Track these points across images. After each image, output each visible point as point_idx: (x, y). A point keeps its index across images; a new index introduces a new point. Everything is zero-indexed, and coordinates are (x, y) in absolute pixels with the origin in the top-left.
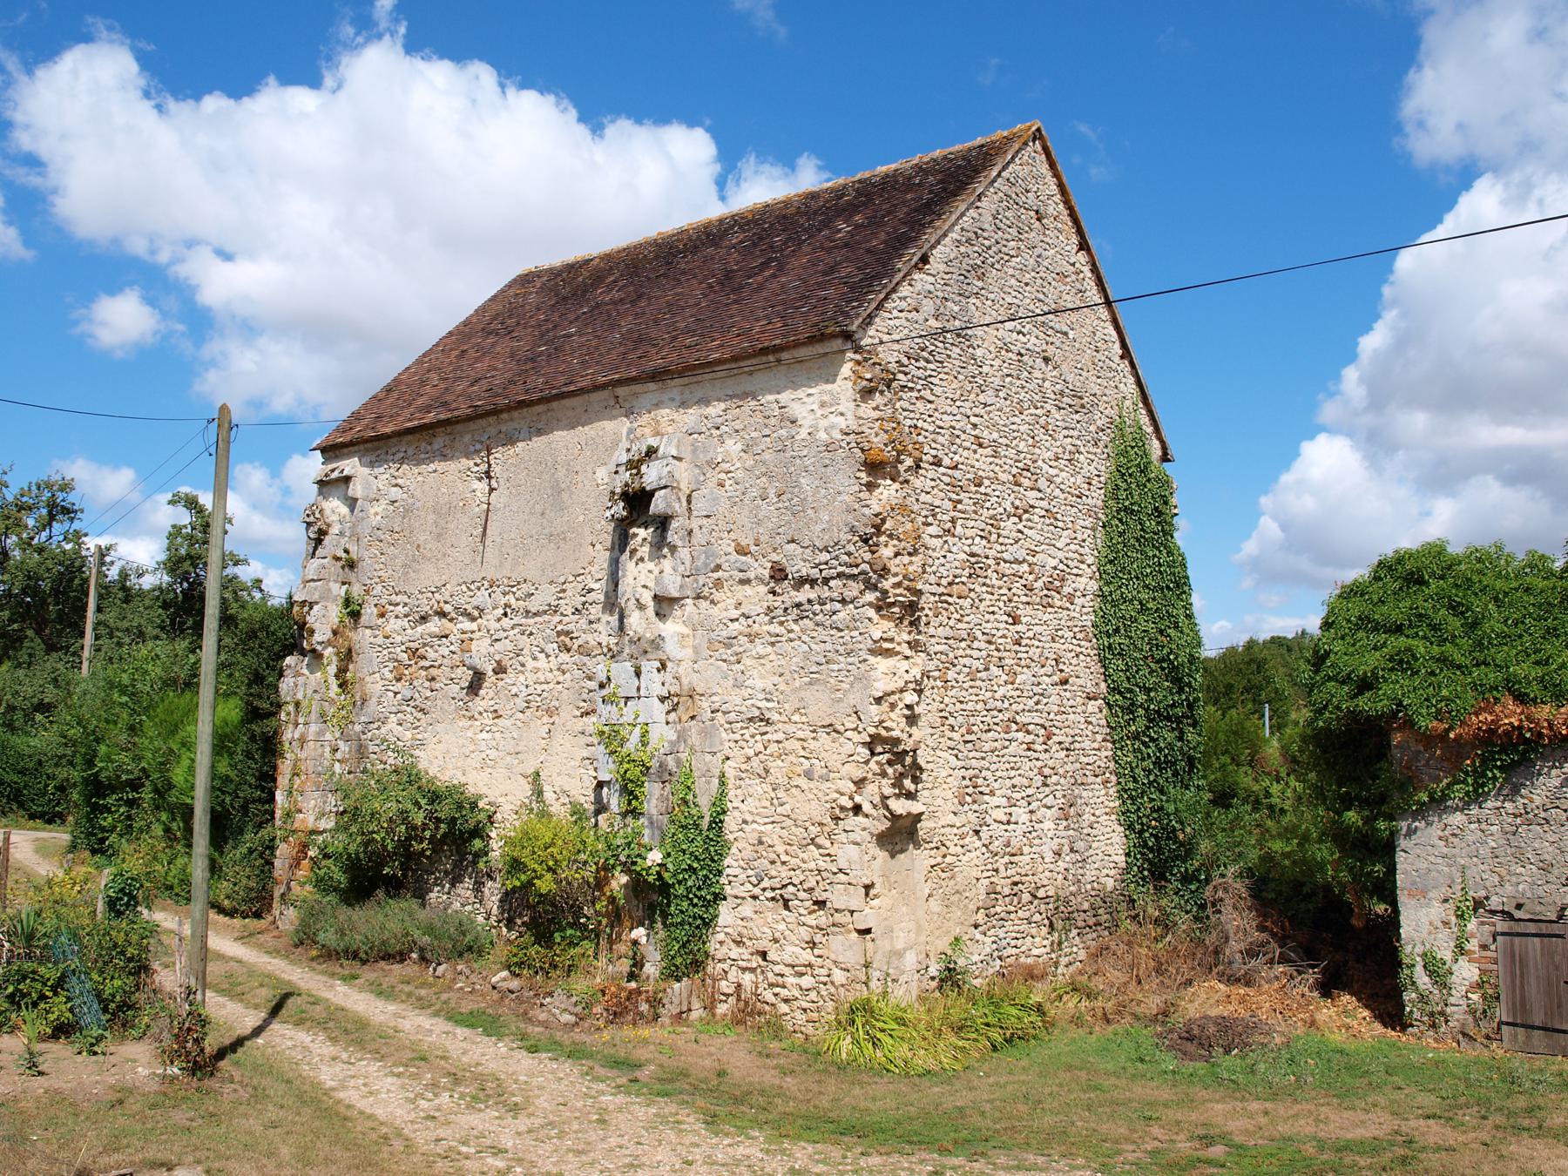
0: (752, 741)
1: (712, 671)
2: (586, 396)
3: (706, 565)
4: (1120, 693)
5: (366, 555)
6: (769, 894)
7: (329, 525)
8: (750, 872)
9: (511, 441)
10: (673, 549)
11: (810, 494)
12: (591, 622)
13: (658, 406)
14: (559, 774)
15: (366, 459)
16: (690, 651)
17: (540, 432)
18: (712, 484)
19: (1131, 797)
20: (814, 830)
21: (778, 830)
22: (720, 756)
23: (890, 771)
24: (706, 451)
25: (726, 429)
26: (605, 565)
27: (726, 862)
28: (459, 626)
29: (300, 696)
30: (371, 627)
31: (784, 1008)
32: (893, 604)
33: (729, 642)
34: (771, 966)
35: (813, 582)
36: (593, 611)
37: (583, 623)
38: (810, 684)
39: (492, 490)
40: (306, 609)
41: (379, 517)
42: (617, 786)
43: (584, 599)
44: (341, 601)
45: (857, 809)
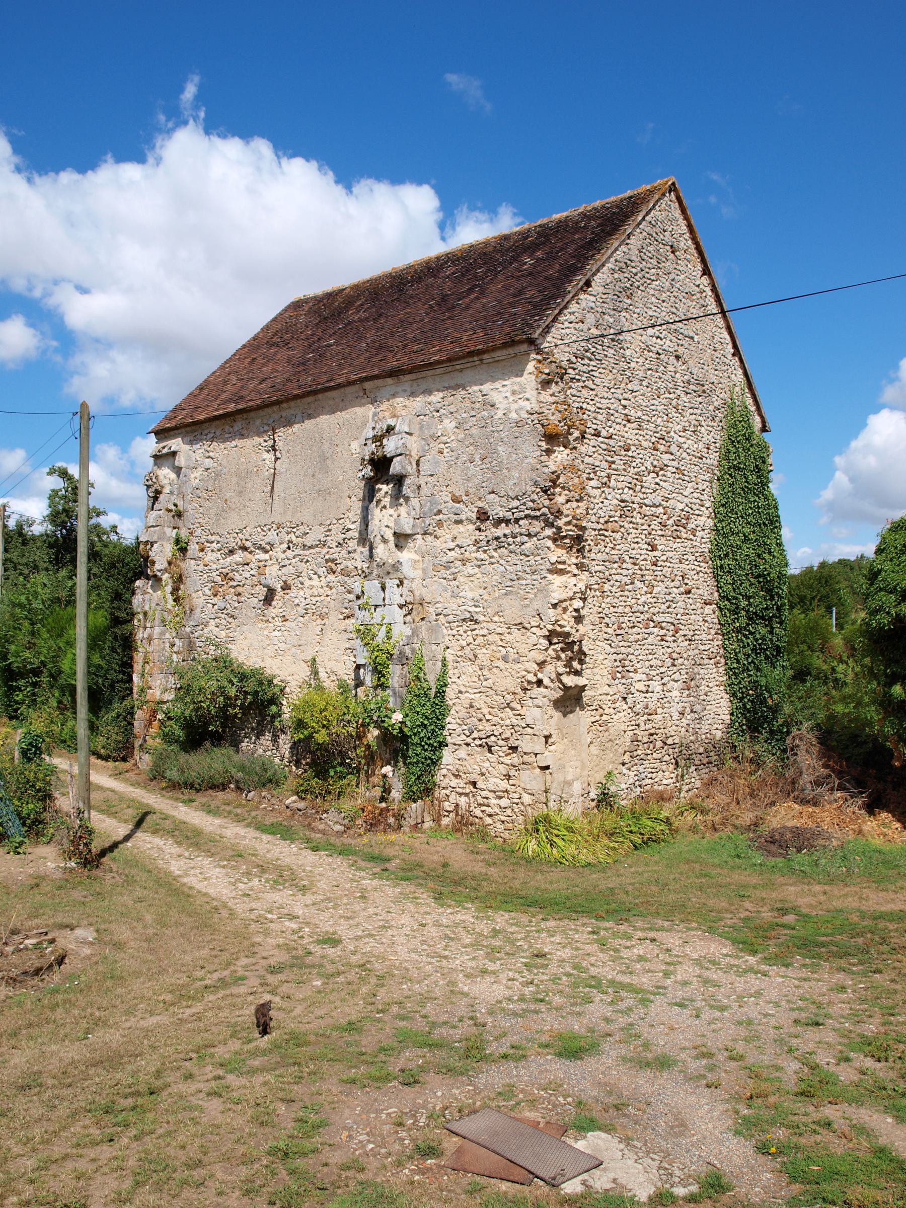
0: (465, 635)
1: (436, 586)
2: (342, 390)
3: (431, 510)
4: (728, 600)
5: (189, 507)
6: (478, 742)
7: (162, 487)
8: (464, 727)
9: (289, 423)
10: (407, 499)
11: (505, 458)
12: (349, 553)
13: (394, 396)
14: (329, 660)
15: (187, 439)
16: (420, 572)
17: (310, 417)
18: (434, 452)
19: (734, 673)
20: (509, 697)
21: (483, 697)
22: (442, 646)
23: (563, 656)
24: (429, 428)
25: (444, 412)
26: (359, 512)
27: (447, 720)
28: (257, 557)
29: (147, 608)
30: (194, 559)
31: (488, 820)
32: (565, 537)
33: (448, 565)
34: (479, 792)
35: (507, 522)
36: (351, 544)
37: (344, 553)
38: (506, 594)
39: (277, 459)
40: (149, 547)
41: (197, 481)
42: (370, 668)
43: (344, 536)
44: (173, 540)
45: (539, 683)
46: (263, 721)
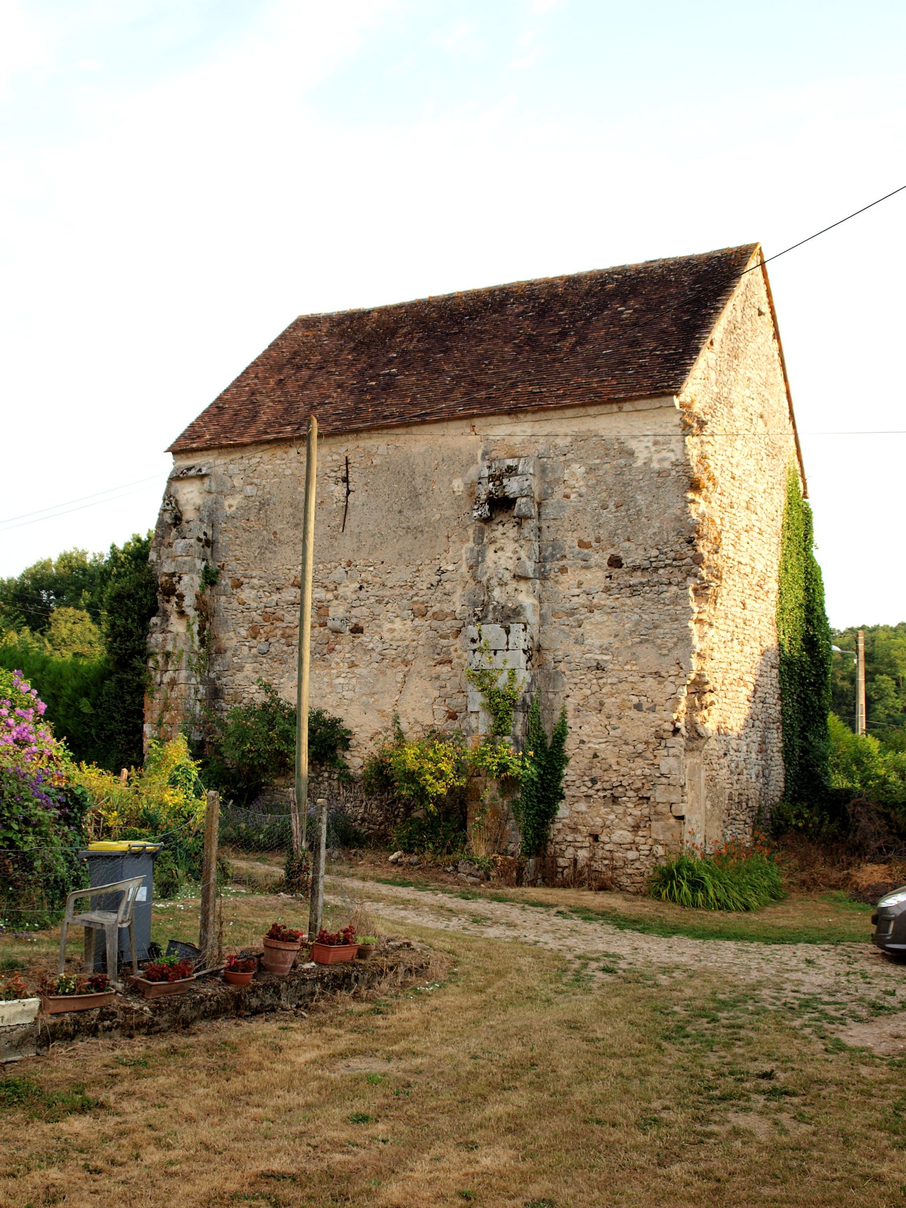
6: (601, 794)
14: (413, 710)
20: (641, 747)
21: (610, 747)
29: (169, 648)
33: (571, 613)
38: (641, 642)
39: (349, 492)
40: (175, 579)
46: (317, 778)
